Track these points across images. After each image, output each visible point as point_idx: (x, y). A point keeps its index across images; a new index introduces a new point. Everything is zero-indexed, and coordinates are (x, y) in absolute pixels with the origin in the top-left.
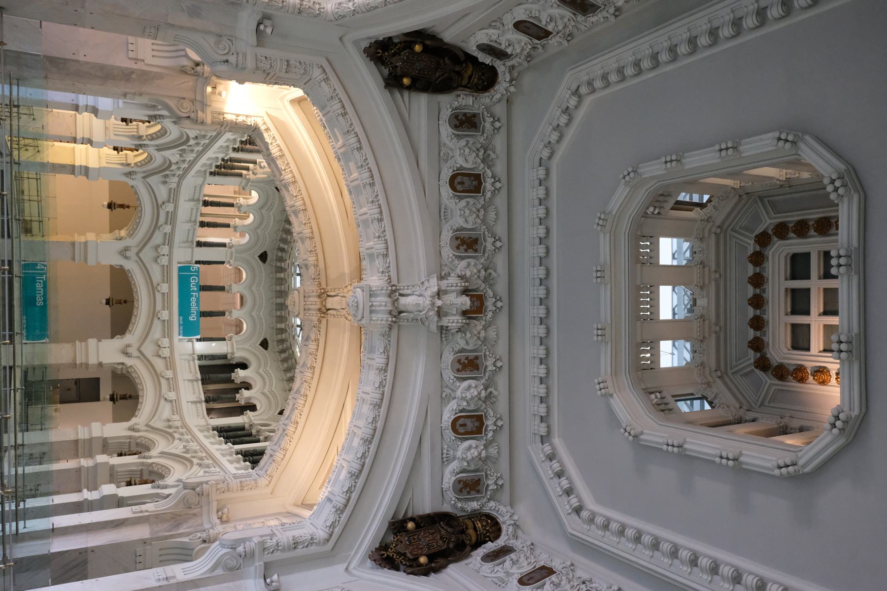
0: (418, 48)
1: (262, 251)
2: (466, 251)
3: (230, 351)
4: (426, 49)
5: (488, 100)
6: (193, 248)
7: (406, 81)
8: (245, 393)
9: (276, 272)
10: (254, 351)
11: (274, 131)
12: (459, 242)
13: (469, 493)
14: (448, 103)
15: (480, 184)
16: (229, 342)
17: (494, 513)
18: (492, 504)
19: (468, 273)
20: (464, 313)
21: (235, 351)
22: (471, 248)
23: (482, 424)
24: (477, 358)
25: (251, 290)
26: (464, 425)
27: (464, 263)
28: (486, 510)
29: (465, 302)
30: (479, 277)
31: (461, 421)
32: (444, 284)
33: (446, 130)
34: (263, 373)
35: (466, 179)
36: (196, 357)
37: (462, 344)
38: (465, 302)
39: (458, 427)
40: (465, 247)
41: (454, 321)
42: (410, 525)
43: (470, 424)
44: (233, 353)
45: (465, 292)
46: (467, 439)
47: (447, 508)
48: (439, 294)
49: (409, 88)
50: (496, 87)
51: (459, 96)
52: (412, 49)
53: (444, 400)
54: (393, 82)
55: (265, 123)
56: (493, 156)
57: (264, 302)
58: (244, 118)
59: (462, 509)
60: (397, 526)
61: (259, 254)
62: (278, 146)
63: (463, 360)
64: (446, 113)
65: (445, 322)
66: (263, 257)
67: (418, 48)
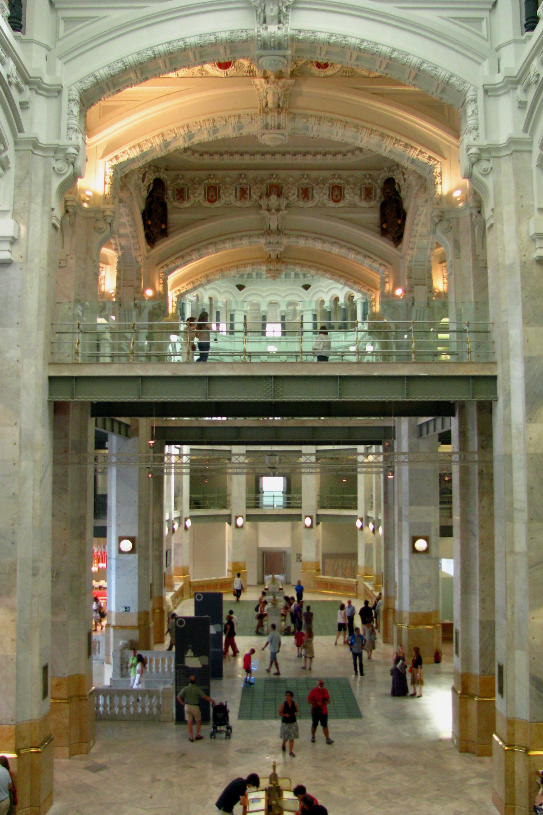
0: (150, 222)
1: (236, 288)
2: (247, 194)
3: (311, 312)
4: (149, 218)
5: (168, 182)
6: (235, 338)
7: (163, 227)
8: (342, 301)
9: (252, 278)
10: (312, 293)
11: (180, 287)
12: (242, 198)
13: (372, 194)
14: (172, 203)
15: (212, 186)
16: (305, 313)
17: (383, 180)
18: (379, 181)
19: (259, 194)
20: (279, 196)
21: (311, 308)
22: (245, 191)
23: (336, 186)
24: (302, 189)
25: (266, 296)
26: (336, 196)
27: (253, 195)
28: (381, 185)
29: (274, 197)
30: (260, 188)
31: (334, 197)
32: (264, 207)
33: (186, 205)
34: (328, 289)
35: (210, 194)
36: (314, 336)
37: (295, 197)
38: (274, 197)
39: (337, 200)
40: (245, 195)
41: (284, 202)
42: (385, 226)
43: (336, 193)
44: (312, 310)
45: (268, 195)
46: (344, 194)
47: (379, 205)
48: (269, 210)
49: (166, 224)
50: (162, 178)
51: (167, 198)
52: (150, 225)
53: (324, 206)
54: (164, 233)
55: (176, 292)
56: (197, 179)
57: (274, 287)
58: (174, 303)
59: (381, 197)
60: (384, 232)
61: (238, 291)
62: (187, 285)
63: (303, 196)
64: (176, 204)
65: (283, 207)
66: (241, 287)
67: (150, 222)
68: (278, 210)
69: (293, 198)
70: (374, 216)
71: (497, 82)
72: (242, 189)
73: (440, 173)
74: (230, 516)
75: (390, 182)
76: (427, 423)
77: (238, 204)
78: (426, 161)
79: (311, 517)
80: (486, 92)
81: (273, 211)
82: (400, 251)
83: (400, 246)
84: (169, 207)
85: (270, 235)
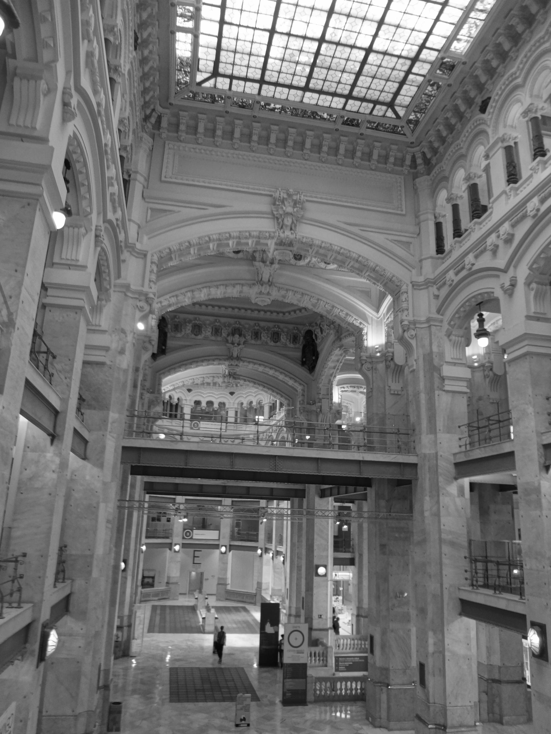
5: (169, 320)
29: (237, 336)
32: (230, 342)
33: (179, 335)
38: (237, 336)
45: (233, 335)
47: (301, 347)
60: (303, 364)
64: (173, 334)
65: (242, 343)
68: (239, 344)
69: (249, 337)
70: (299, 354)
71: (420, 281)
72: (216, 329)
73: (367, 333)
74: (171, 544)
75: (309, 333)
76: (331, 488)
77: (213, 338)
78: (358, 324)
79: (226, 546)
80: (413, 286)
81: (236, 345)
82: (313, 376)
83: (313, 373)
84: (169, 335)
85: (232, 360)
